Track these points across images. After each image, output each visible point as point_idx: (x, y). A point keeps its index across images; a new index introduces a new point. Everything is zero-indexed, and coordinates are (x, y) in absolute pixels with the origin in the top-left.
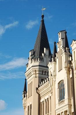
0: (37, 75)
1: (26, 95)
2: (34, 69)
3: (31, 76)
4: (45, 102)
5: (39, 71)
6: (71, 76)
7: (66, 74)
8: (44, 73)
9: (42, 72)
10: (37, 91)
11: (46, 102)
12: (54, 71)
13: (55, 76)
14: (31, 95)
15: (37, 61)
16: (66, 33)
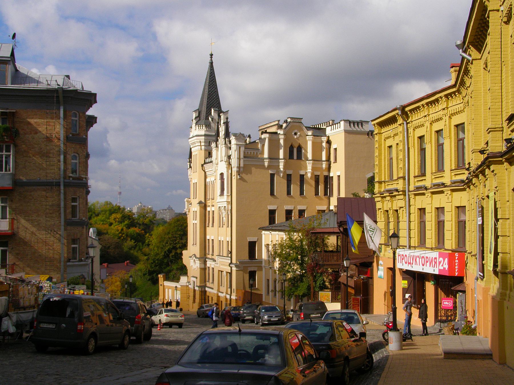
0: (203, 147)
3: (196, 146)
5: (205, 142)
6: (230, 172)
10: (202, 168)
11: (212, 184)
12: (216, 159)
13: (217, 164)
15: (203, 128)
16: (227, 119)
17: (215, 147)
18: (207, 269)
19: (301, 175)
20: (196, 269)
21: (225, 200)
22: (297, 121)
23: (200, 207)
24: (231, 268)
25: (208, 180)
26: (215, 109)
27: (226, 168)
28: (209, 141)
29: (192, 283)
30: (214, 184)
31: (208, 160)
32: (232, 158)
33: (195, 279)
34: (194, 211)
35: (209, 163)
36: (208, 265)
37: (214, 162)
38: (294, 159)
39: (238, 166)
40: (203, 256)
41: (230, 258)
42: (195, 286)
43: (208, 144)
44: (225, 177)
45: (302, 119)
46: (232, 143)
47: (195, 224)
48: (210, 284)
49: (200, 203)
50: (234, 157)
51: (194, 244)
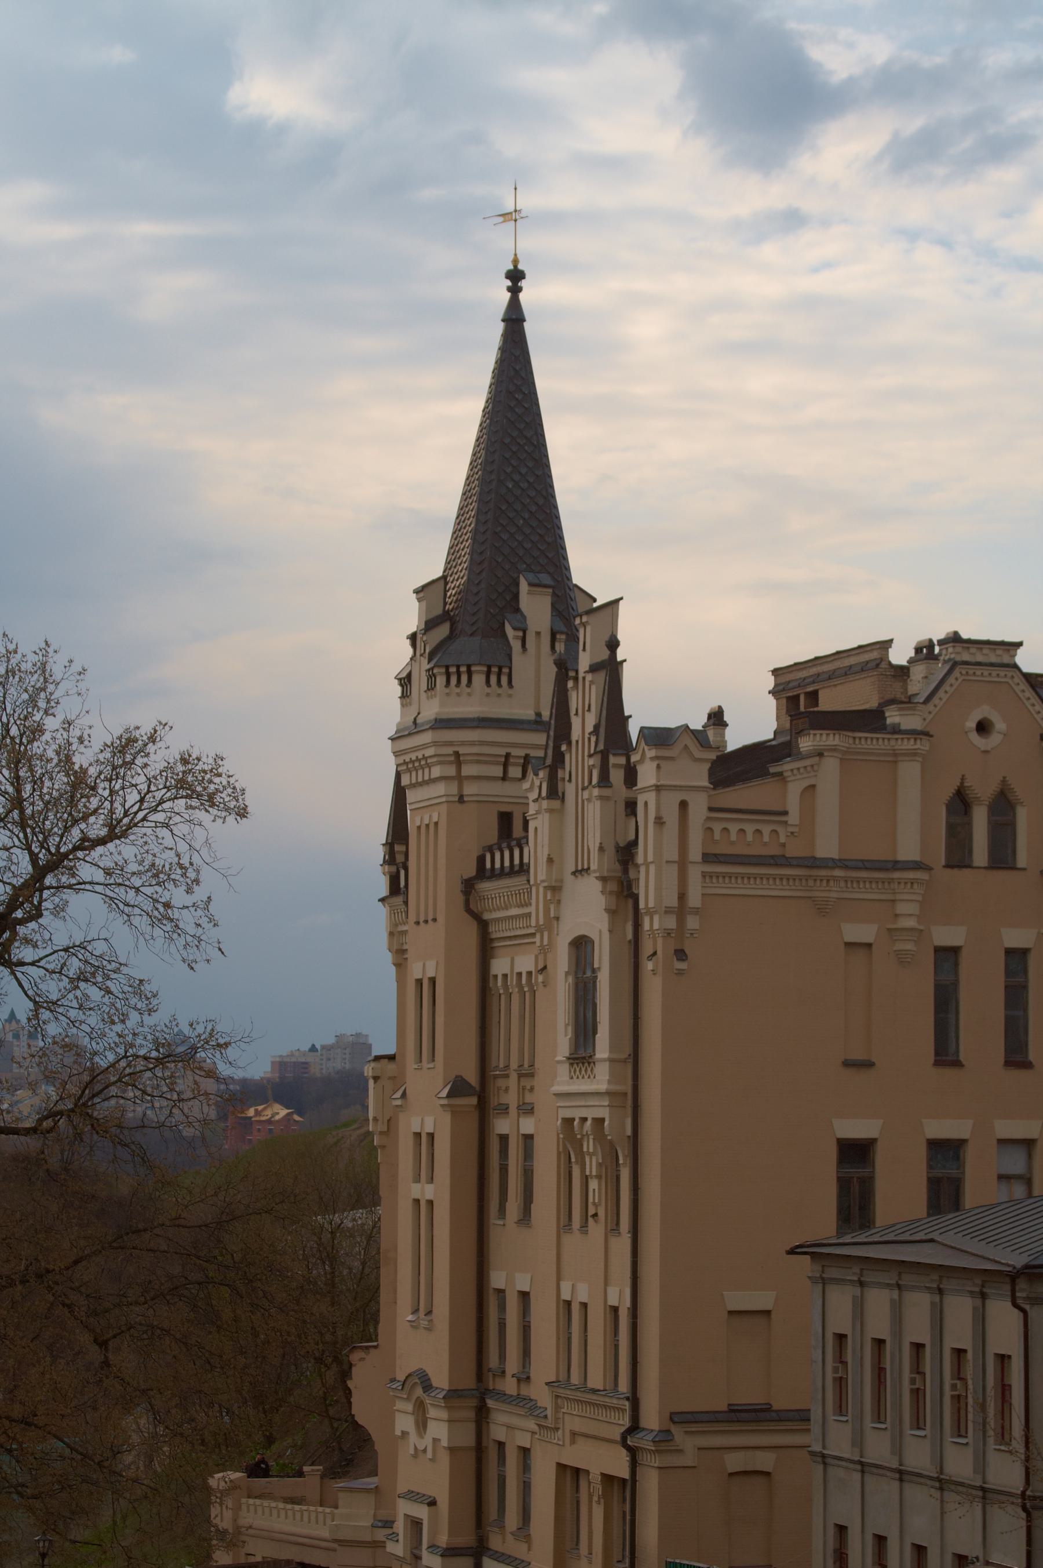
1: (402, 873)
2: (450, 744)
4: (517, 990)
6: (630, 936)
7: (605, 917)
8: (515, 772)
9: (505, 766)
10: (467, 903)
12: (550, 860)
14: (430, 918)
16: (613, 644)
17: (544, 793)
18: (492, 1454)
19: (1009, 952)
20: (429, 1455)
21: (603, 1087)
22: (993, 659)
23: (454, 1114)
24: (633, 1452)
25: (499, 966)
26: (531, 576)
27: (607, 910)
28: (503, 752)
29: (400, 1526)
30: (534, 993)
31: (501, 860)
32: (640, 859)
33: (422, 1512)
34: (418, 1135)
35: (502, 874)
36: (497, 1432)
37: (539, 872)
38: (976, 864)
39: (674, 903)
40: (469, 1382)
41: (627, 1403)
42: (425, 1545)
43: (501, 768)
44: (602, 958)
45: (1019, 644)
46: (640, 784)
47: (423, 1204)
48: (509, 1538)
49: (458, 1088)
50: (650, 859)
51: (416, 1311)
